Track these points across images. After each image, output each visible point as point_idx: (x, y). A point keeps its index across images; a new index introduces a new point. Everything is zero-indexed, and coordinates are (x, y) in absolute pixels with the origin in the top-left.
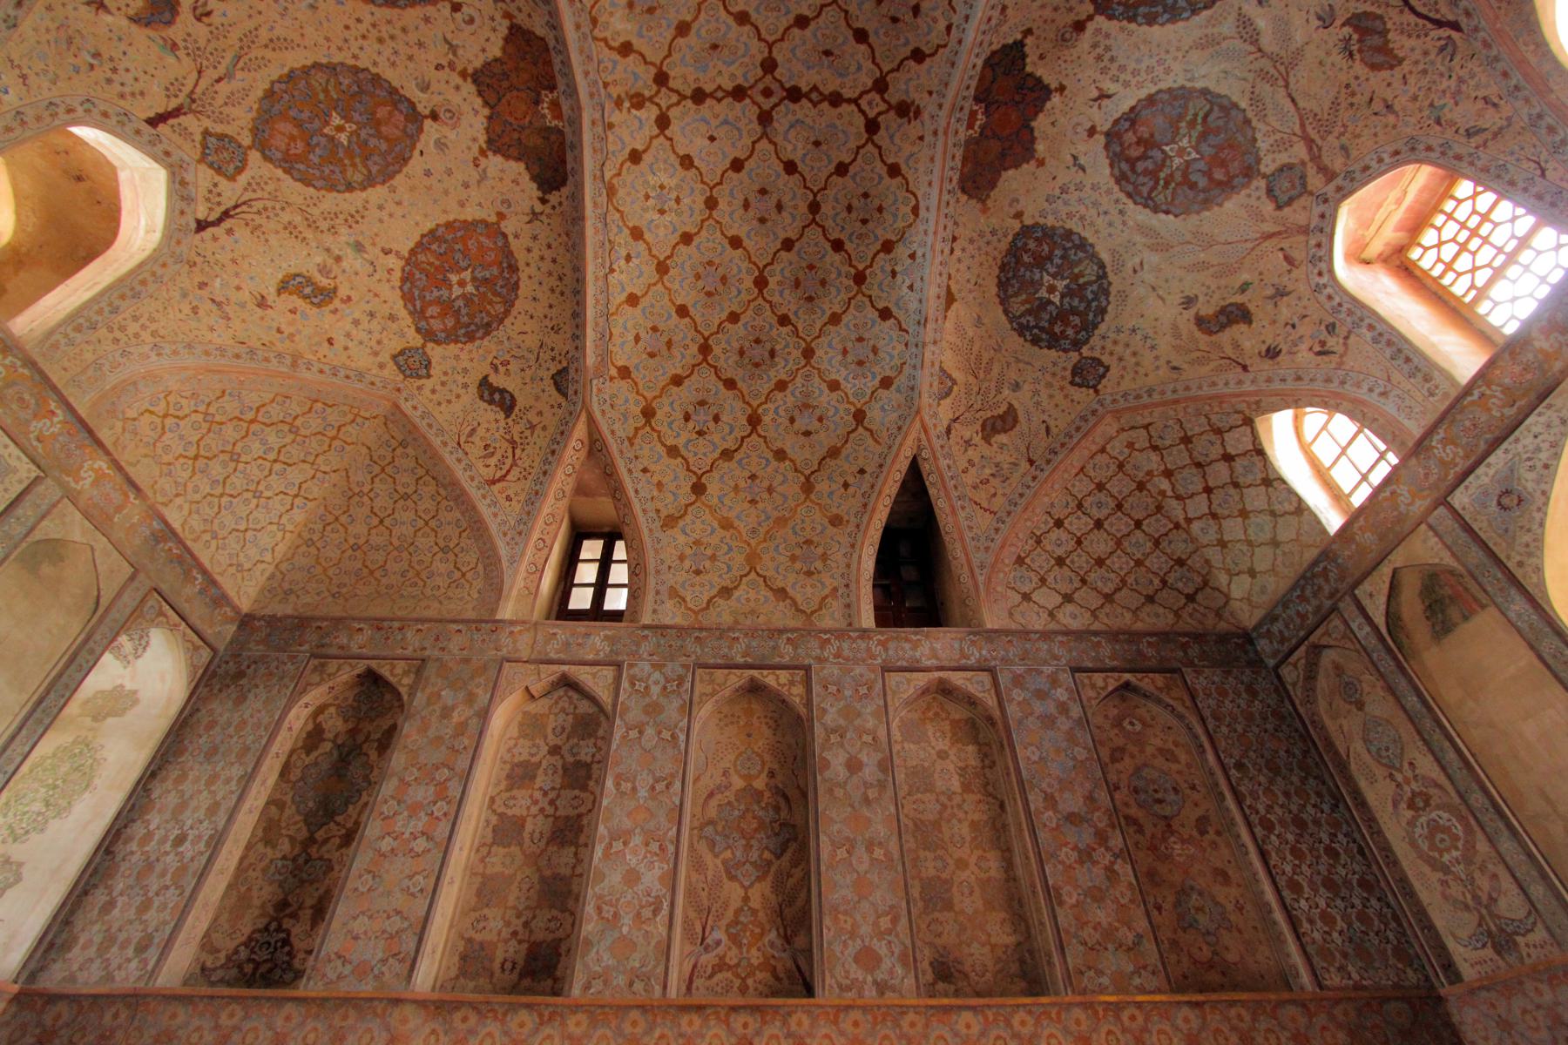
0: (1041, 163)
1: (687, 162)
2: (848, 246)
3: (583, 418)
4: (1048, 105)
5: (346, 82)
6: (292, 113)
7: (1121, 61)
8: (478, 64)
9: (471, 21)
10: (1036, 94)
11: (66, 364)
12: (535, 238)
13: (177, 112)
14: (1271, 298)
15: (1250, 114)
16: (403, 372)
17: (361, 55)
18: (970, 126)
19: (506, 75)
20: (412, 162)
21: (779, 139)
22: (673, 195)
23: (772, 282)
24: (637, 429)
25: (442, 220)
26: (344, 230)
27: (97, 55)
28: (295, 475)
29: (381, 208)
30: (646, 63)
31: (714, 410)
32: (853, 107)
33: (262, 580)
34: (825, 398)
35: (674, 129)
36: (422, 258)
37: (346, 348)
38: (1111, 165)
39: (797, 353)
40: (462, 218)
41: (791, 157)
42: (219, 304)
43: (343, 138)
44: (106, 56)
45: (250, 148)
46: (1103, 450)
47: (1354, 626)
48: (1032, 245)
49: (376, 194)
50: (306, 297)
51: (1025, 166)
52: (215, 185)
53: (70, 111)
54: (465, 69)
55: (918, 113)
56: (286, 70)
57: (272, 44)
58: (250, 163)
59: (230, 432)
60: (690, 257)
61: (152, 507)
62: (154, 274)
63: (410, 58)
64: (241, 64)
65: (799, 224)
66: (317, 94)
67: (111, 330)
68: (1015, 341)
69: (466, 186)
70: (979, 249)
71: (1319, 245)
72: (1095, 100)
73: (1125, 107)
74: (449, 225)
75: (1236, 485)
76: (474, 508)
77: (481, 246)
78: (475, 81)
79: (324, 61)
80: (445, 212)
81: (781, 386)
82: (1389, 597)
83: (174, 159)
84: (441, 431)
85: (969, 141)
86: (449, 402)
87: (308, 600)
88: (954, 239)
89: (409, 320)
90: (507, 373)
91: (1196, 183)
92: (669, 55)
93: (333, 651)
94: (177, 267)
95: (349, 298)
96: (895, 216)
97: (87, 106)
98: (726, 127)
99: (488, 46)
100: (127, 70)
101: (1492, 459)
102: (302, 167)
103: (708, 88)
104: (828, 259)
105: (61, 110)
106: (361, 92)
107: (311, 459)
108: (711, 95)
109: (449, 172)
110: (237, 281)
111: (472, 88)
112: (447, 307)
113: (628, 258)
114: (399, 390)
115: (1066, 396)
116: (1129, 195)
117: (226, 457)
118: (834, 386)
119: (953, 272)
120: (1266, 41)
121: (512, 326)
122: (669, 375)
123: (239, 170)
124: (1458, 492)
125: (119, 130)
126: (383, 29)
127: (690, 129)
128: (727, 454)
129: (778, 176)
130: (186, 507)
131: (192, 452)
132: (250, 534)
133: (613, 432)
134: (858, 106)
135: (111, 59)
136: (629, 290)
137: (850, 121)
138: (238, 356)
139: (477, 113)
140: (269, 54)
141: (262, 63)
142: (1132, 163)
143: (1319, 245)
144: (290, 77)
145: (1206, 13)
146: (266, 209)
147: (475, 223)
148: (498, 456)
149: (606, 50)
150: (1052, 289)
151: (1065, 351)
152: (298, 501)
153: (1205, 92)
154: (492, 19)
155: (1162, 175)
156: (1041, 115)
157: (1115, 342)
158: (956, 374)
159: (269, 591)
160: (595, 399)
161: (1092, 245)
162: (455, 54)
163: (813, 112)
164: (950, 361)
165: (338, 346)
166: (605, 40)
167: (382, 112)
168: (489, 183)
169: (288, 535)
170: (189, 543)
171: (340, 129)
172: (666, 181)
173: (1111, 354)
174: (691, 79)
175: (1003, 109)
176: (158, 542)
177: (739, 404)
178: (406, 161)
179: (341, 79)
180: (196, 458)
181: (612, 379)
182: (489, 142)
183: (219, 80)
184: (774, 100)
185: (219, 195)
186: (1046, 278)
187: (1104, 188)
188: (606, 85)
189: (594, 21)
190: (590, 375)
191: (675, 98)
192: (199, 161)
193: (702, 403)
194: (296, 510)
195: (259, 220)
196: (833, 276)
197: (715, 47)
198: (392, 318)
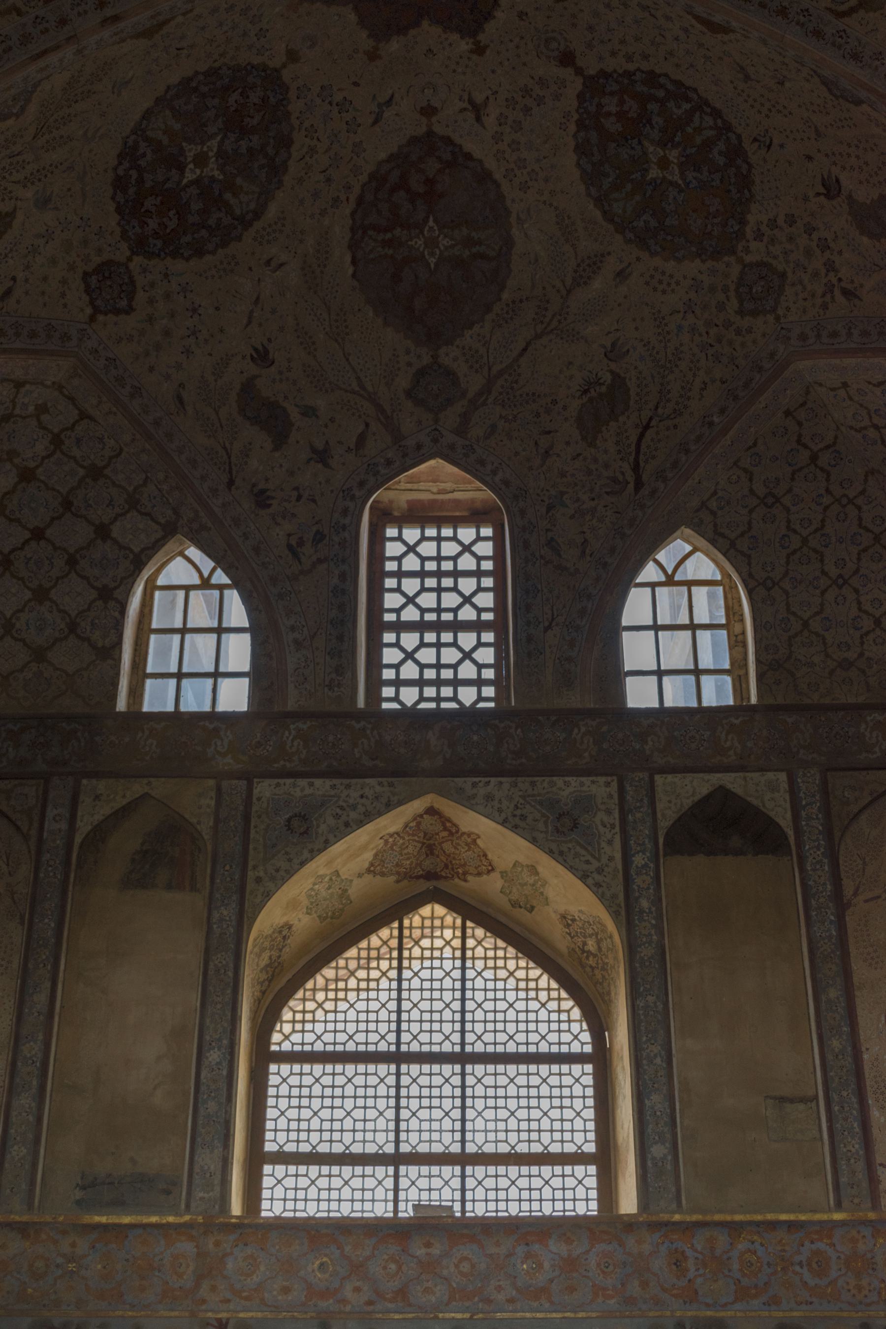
0: (373, 56)
4: (455, 37)
14: (314, 450)
46: (19, 385)
47: (50, 813)
51: (364, 34)
71: (389, 462)
72: (471, 101)
73: (469, 146)
75: (72, 562)
82: (115, 813)
101: (318, 782)
115: (64, 282)
116: (360, 201)
124: (267, 782)
143: (389, 462)
145: (598, 214)
150: (201, 160)
151: (124, 235)
155: (398, 231)
157: (167, 296)
173: (151, 301)
186: (214, 143)
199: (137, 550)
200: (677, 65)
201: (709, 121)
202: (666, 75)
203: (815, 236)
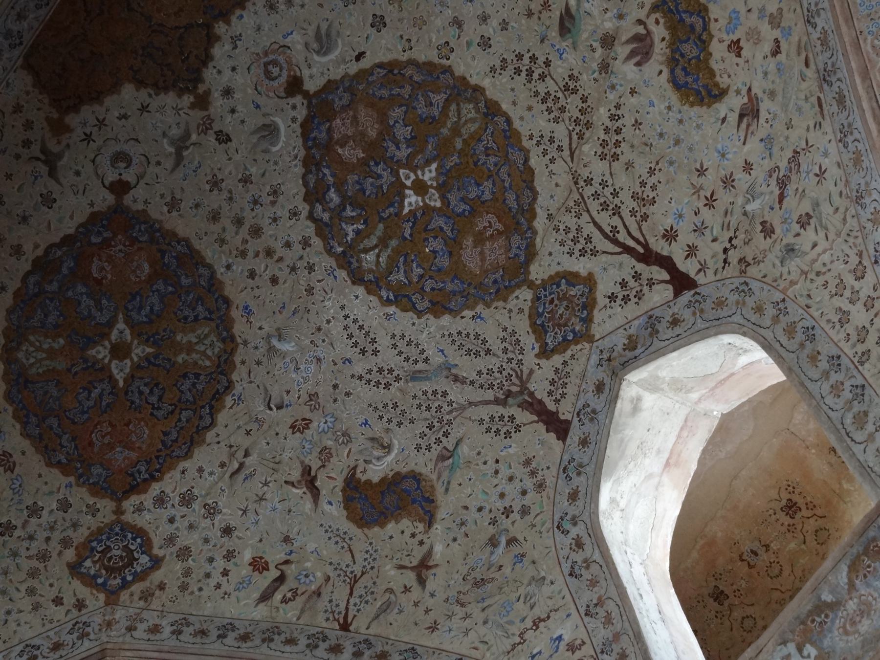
5: (350, 229)
6: (444, 262)
8: (170, 99)
9: (121, 157)
17: (295, 238)
20: (385, 57)
26: (560, 70)
27: (493, 542)
29: (485, 43)
42: (783, 184)
43: (429, 175)
44: (492, 530)
45: (531, 285)
49: (472, 66)
50: (703, 44)
52: (612, 297)
54: (193, 106)
56: (392, 309)
57: (367, 347)
58: (555, 269)
62: (776, 320)
63: (246, 180)
64: (420, 366)
66: (397, 252)
78: (198, 79)
79: (343, 274)
83: (602, 374)
94: (755, 285)
97: (567, 525)
100: (502, 495)
102: (511, 197)
105: (579, 557)
111: (209, 74)
123: (572, 278)
125: (589, 469)
126: (239, 238)
135: (493, 522)
139: (235, 40)
140: (384, 342)
141: (402, 345)
146: (605, 206)
154: (88, 138)
162: (187, 135)
178: (391, 68)
179: (351, 235)
183: (456, 379)
185: (624, 284)
192: (591, 339)
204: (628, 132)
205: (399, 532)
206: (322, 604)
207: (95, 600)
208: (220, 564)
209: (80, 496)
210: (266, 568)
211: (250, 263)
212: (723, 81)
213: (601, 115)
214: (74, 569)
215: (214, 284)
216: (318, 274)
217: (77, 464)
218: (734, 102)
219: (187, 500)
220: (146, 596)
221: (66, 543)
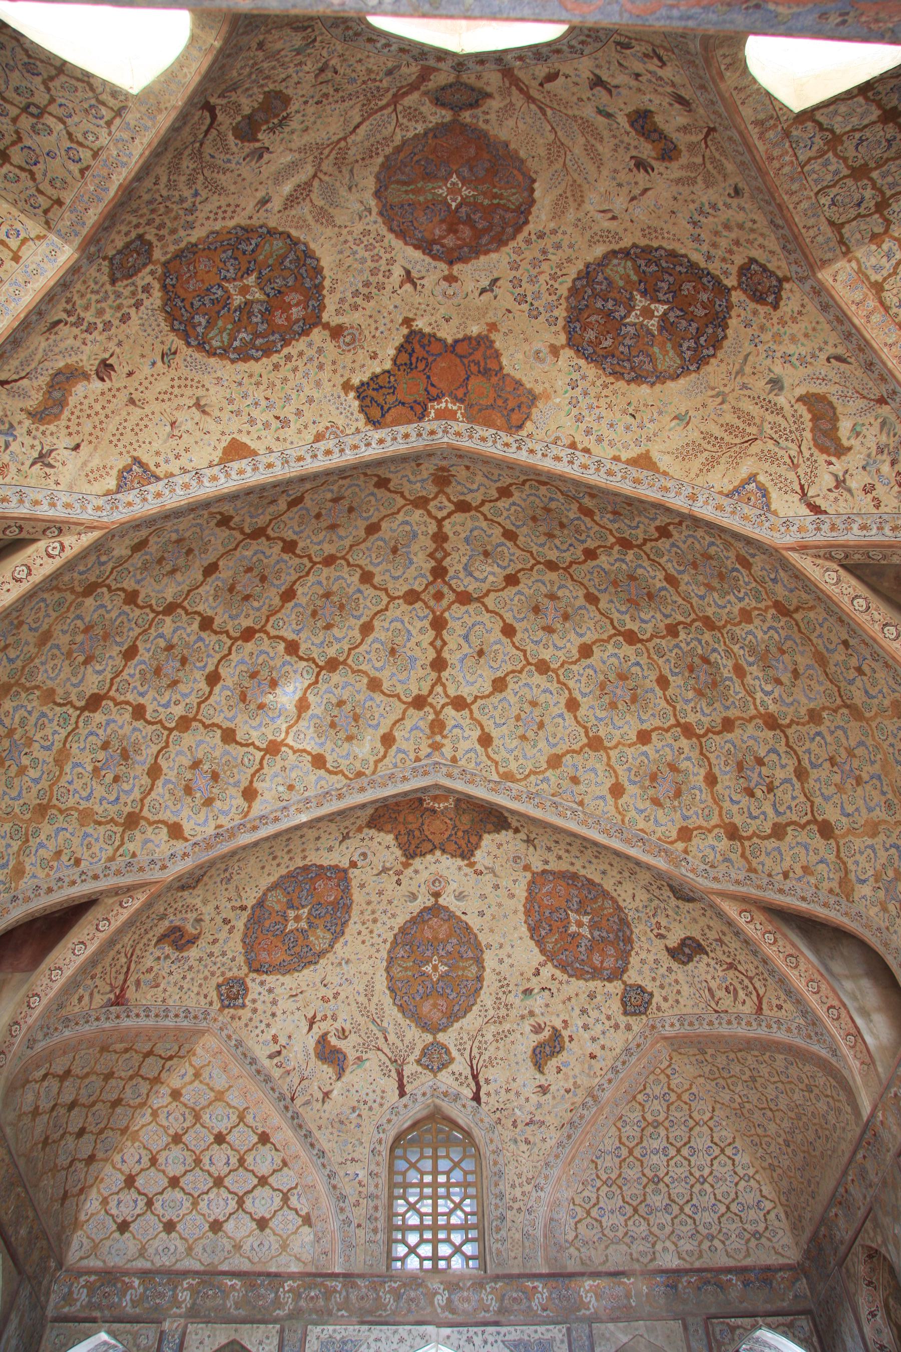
0: (493, 327)
1: (499, 685)
2: (591, 544)
3: (718, 900)
4: (427, 330)
7: (366, 275)
8: (398, 853)
9: (364, 855)
10: (417, 349)
11: (513, 1254)
12: (549, 849)
13: (400, 1075)
15: (388, 150)
16: (640, 1013)
17: (384, 936)
18: (452, 415)
19: (410, 833)
20: (470, 923)
21: (485, 587)
22: (526, 707)
23: (630, 625)
24: (743, 855)
25: (523, 918)
26: (511, 998)
28: (701, 1142)
29: (501, 961)
30: (403, 719)
31: (750, 759)
32: (446, 523)
33: (785, 1224)
34: (758, 632)
35: (466, 692)
36: (549, 946)
37: (603, 1047)
38: (486, 253)
39: (707, 636)
40: (523, 901)
41: (501, 578)
43: (443, 968)
48: (591, 335)
50: (553, 1054)
51: (497, 345)
53: (380, 1142)
55: (443, 469)
57: (369, 995)
59: (632, 1173)
60: (592, 707)
61: (642, 1273)
62: (494, 1152)
63: (390, 902)
65: (569, 584)
67: (511, 1208)
68: (715, 371)
69: (496, 887)
70: (590, 408)
72: (415, 285)
74: (528, 913)
76: (777, 1043)
77: (549, 894)
78: (413, 857)
79: (385, 964)
80: (515, 912)
81: (739, 671)
84: (700, 1018)
85: (470, 418)
86: (679, 992)
87: (808, 1216)
88: (573, 446)
89: (598, 983)
90: (668, 929)
91: (487, 170)
92: (398, 696)
93: (843, 1249)
95: (565, 1022)
96: (551, 499)
98: (472, 638)
99: (384, 844)
102: (457, 1008)
103: (432, 654)
104: (606, 567)
106: (411, 944)
107: (691, 1123)
108: (439, 652)
109: (483, 897)
110: (522, 1098)
112: (594, 945)
113: (575, 780)
114: (653, 1027)
116: (518, 229)
117: (651, 1187)
118: (746, 616)
119: (611, 453)
120: (303, 176)
121: (627, 903)
122: (703, 786)
123: (448, 1052)
127: (466, 680)
128: (801, 774)
129: (519, 593)
130: (668, 1244)
131: (629, 1210)
132: (734, 1207)
133: (737, 882)
134: (444, 519)
136: (604, 790)
137: (458, 526)
138: (569, 1137)
140: (375, 1000)
142: (478, 234)
143: (521, 58)
144: (392, 990)
145: (294, 233)
147: (530, 891)
148: (739, 987)
149: (386, 761)
150: (647, 313)
152: (729, 1151)
153: (377, 194)
156: (439, 335)
157: (714, 245)
158: (744, 471)
159: (796, 1228)
160: (700, 880)
161: (588, 266)
163: (455, 555)
164: (722, 479)
165: (599, 1053)
166: (376, 762)
167: (428, 934)
168: (498, 869)
169: (757, 1177)
170: (697, 1265)
171: (435, 968)
172: (515, 711)
174: (422, 673)
175: (435, 380)
176: (674, 1287)
177: (750, 729)
178: (468, 927)
180: (636, 1210)
181: (686, 852)
182: (463, 857)
184: (446, 590)
186: (632, 319)
187: (514, 257)
188: (418, 759)
189: (360, 774)
190: (676, 872)
191: (439, 689)
193: (740, 767)
194: (737, 1158)
195: (486, 1056)
196: (624, 566)
197: (393, 652)
198: (592, 996)
199: (861, 99)
200: (251, 376)
201: (215, 343)
202: (257, 360)
203: (100, 326)
204: (508, 1040)
205: (327, 1071)
206: (288, 1080)
207: (217, 1005)
208: (263, 1026)
209: (241, 959)
210: (276, 1042)
211: (363, 929)
212: (546, 1071)
213: (507, 1026)
214: (219, 986)
215: (345, 924)
216: (378, 955)
217: (249, 946)
218: (542, 1080)
219: (270, 991)
220: (233, 1018)
221: (223, 974)
